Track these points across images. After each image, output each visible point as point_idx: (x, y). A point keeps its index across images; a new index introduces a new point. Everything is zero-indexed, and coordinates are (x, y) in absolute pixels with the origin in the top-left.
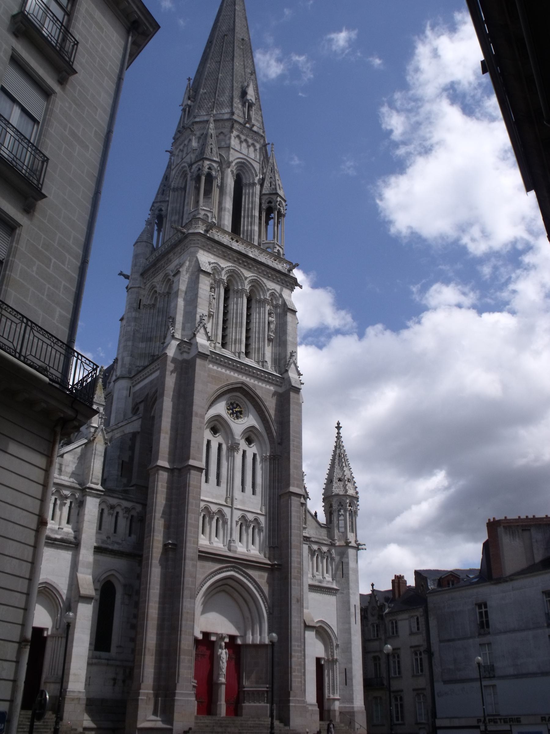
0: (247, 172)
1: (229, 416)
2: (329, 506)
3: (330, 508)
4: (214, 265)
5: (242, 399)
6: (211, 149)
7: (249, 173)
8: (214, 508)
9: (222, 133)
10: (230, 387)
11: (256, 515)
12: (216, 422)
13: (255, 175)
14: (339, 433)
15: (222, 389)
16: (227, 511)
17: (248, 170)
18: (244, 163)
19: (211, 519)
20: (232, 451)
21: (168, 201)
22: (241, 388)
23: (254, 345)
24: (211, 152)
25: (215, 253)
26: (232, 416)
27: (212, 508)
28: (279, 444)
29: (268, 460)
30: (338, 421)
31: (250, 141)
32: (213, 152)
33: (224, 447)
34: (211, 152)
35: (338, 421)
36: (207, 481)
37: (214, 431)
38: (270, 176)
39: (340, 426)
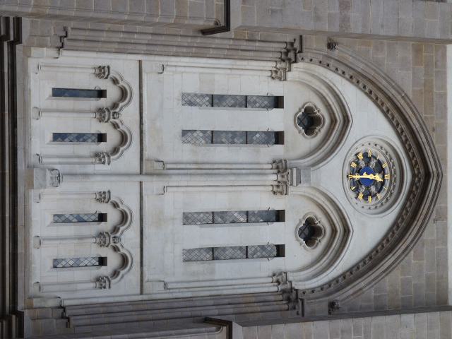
1: (352, 158)
5: (399, 192)
8: (128, 115)
10: (422, 139)
11: (137, 259)
12: (327, 121)
15: (410, 113)
16: (129, 157)
19: (101, 114)
20: (276, 171)
22: (428, 175)
26: (354, 165)
27: (125, 109)
28: (332, 305)
29: (281, 287)
33: (278, 151)
36: (190, 101)
37: (309, 121)
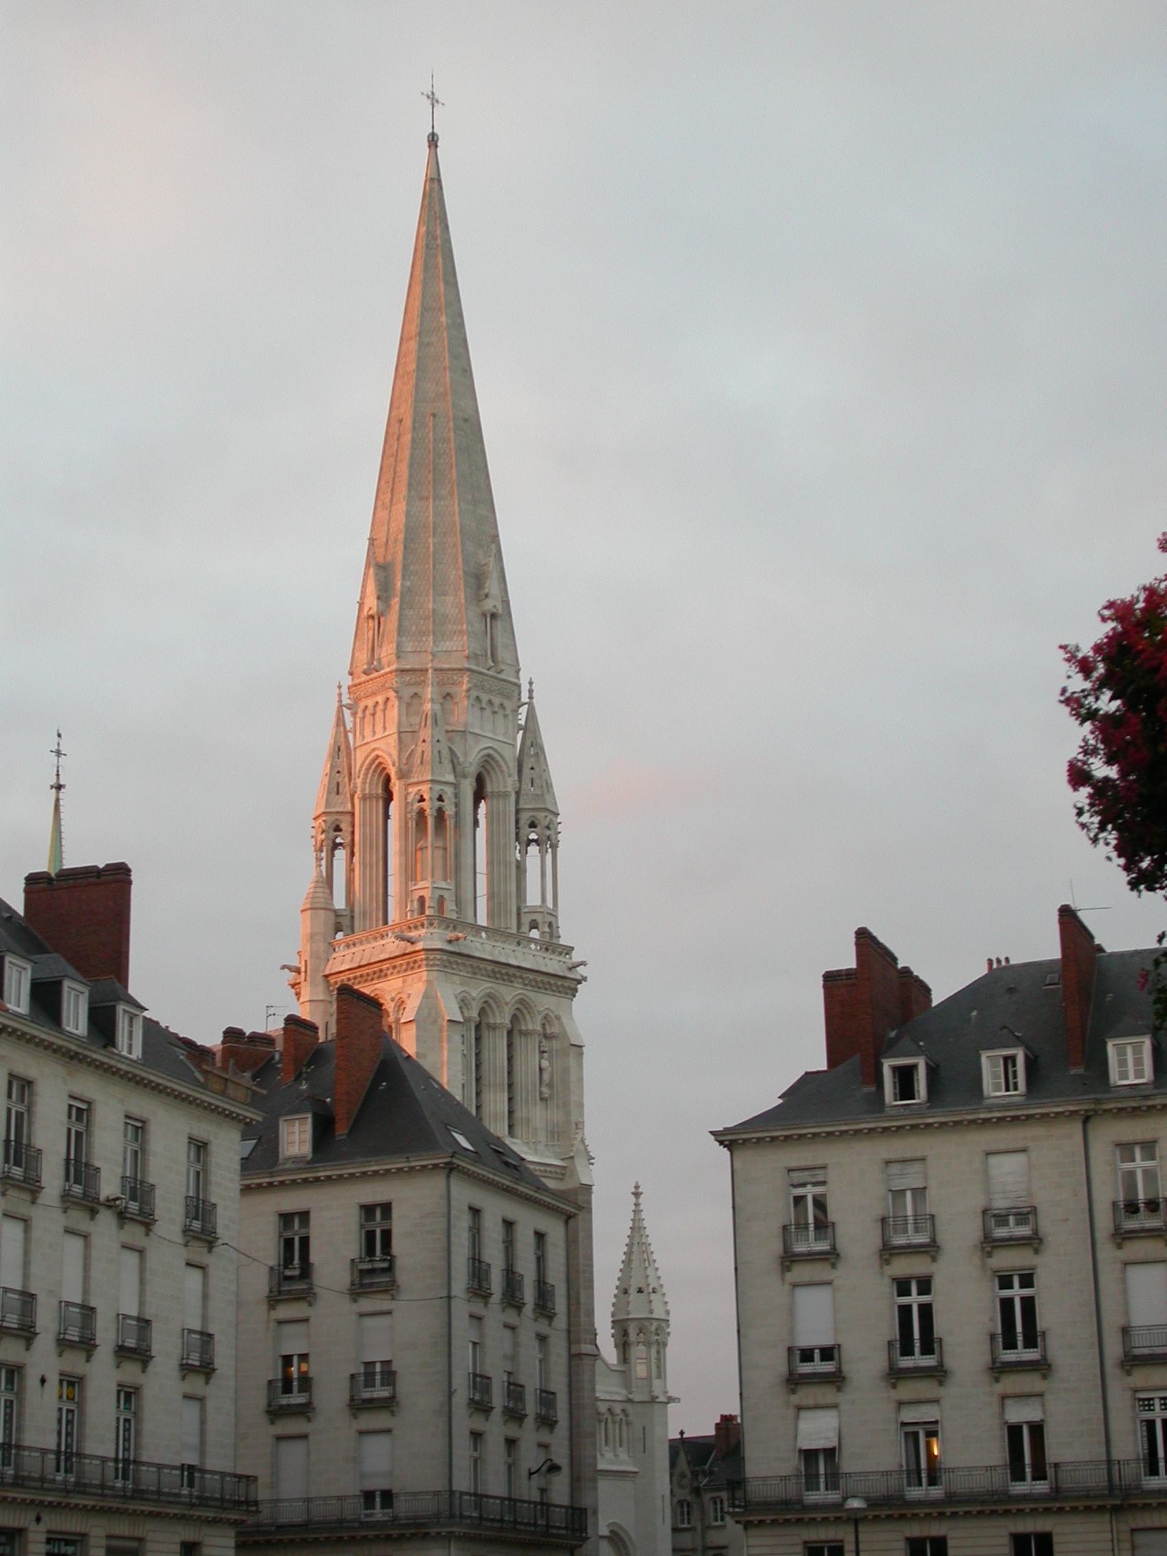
0: (493, 768)
2: (623, 1333)
3: (624, 1336)
4: (463, 994)
6: (439, 752)
7: (498, 771)
9: (448, 694)
13: (506, 775)
14: (637, 1205)
17: (495, 766)
18: (489, 755)
21: (353, 814)
23: (520, 1113)
24: (440, 763)
25: (462, 973)
30: (637, 1183)
31: (497, 701)
32: (443, 760)
34: (440, 763)
35: (637, 1183)
38: (530, 766)
39: (640, 1190)
